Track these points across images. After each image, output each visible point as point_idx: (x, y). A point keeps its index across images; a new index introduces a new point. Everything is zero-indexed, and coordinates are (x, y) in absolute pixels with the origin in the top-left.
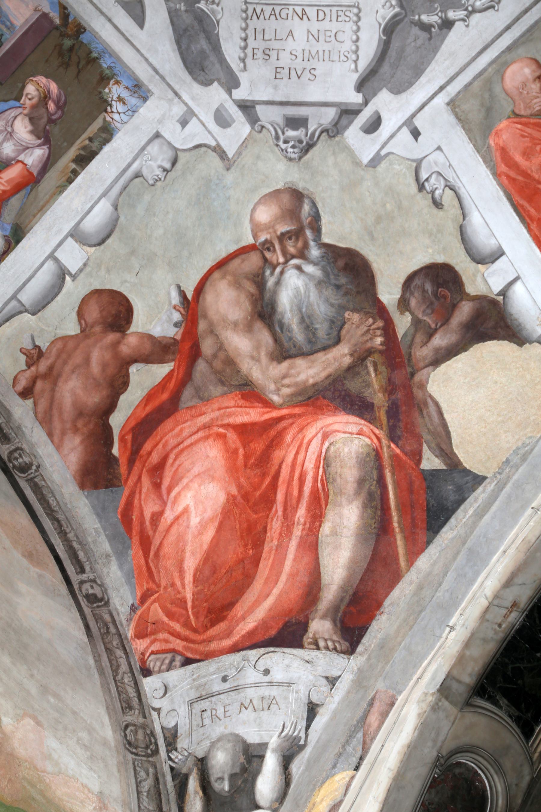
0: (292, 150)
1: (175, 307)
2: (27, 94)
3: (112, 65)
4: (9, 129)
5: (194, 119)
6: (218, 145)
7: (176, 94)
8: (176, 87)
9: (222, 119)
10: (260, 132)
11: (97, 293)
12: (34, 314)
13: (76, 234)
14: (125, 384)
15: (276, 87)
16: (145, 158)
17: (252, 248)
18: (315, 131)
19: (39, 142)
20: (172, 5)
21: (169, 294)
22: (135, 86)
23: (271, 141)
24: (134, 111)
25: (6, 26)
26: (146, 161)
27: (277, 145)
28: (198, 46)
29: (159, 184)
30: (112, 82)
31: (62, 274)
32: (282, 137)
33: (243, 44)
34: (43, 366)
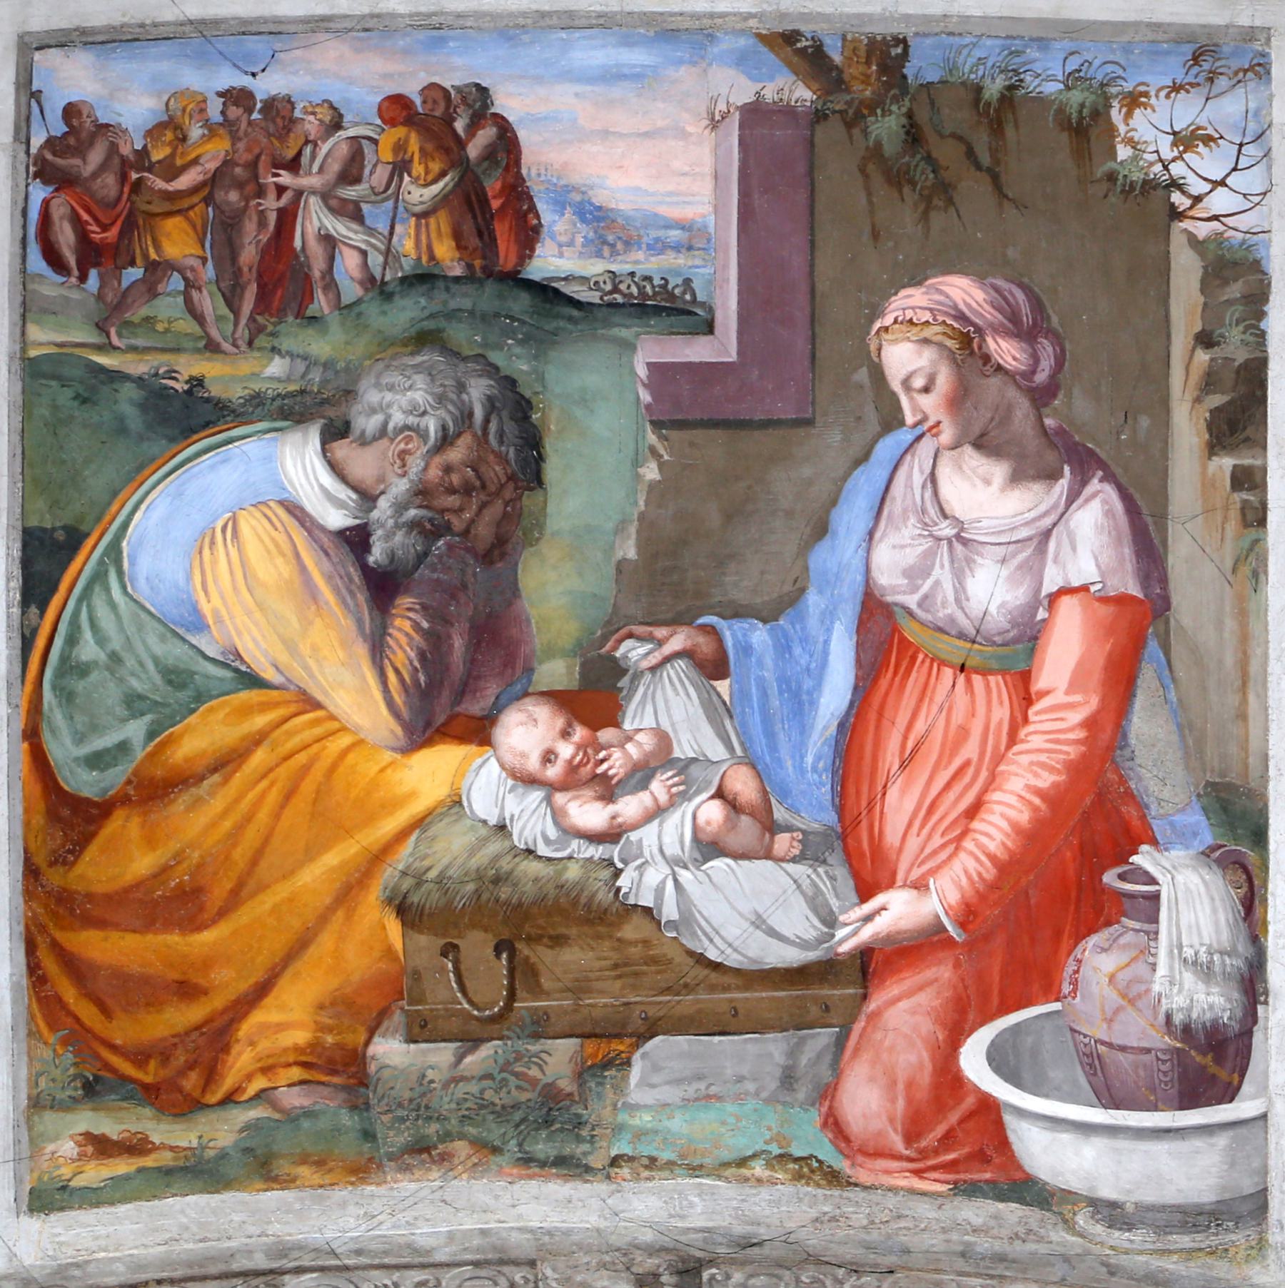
2: (906, 383)
3: (1072, 64)
4: (946, 530)
19: (1063, 484)
22: (1196, 59)
25: (677, 248)
30: (1116, 115)
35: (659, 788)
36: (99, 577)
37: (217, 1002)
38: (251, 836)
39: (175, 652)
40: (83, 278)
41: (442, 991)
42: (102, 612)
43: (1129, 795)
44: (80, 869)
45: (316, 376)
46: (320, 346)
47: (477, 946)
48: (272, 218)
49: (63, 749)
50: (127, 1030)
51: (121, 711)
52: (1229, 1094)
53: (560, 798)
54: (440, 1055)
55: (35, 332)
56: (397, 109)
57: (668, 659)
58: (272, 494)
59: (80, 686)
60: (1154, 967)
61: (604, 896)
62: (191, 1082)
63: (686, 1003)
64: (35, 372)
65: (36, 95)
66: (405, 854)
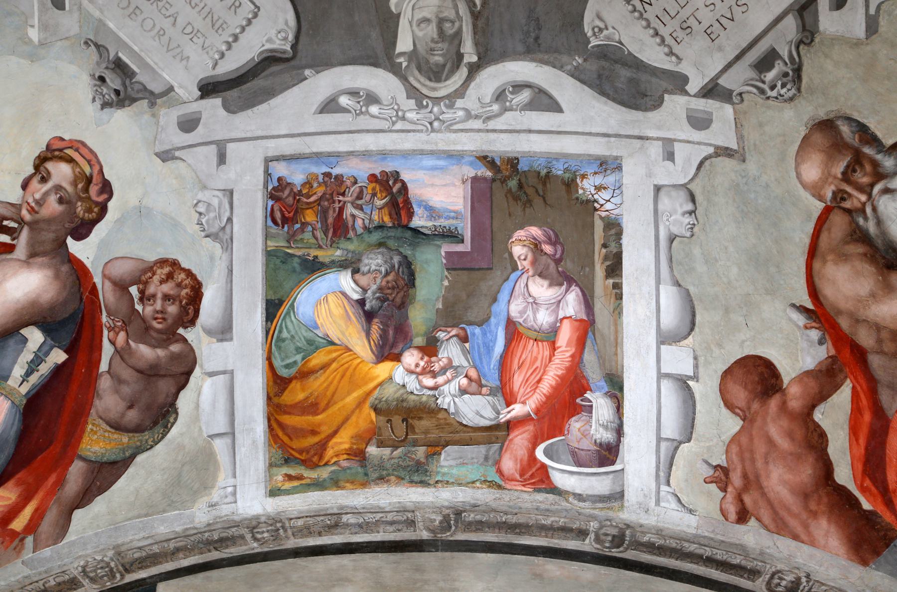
0: (785, 90)
1: (806, 328)
2: (519, 258)
3: (566, 166)
5: (676, 144)
6: (717, 148)
7: (640, 138)
8: (636, 133)
9: (700, 122)
10: (742, 100)
11: (727, 373)
12: (689, 441)
13: (665, 339)
14: (823, 435)
15: (720, 49)
16: (665, 219)
17: (827, 212)
18: (790, 52)
19: (564, 287)
20: (569, 67)
21: (790, 320)
22: (601, 165)
23: (760, 100)
24: (619, 188)
25: (453, 218)
26: (668, 220)
27: (768, 98)
28: (622, 79)
29: (696, 229)
30: (578, 181)
31: (683, 383)
32: (766, 87)
33: (658, 40)
34: (736, 479)
35: (449, 374)
36: (288, 313)
37: (323, 436)
38: (332, 389)
39: (310, 335)
40: (283, 227)
41: (387, 433)
42: (289, 324)
43: (584, 377)
44: (283, 398)
45: (350, 255)
46: (351, 247)
47: (397, 420)
48: (337, 209)
49: (278, 363)
50: (297, 444)
51: (294, 352)
52: (613, 463)
53: (420, 377)
54: (387, 451)
55: (269, 243)
56: (373, 178)
57: (451, 337)
58: (338, 289)
59: (283, 345)
60: (591, 426)
61: (433, 406)
62: (315, 459)
63: (457, 436)
64: (269, 255)
65: (270, 175)
66: (376, 394)
